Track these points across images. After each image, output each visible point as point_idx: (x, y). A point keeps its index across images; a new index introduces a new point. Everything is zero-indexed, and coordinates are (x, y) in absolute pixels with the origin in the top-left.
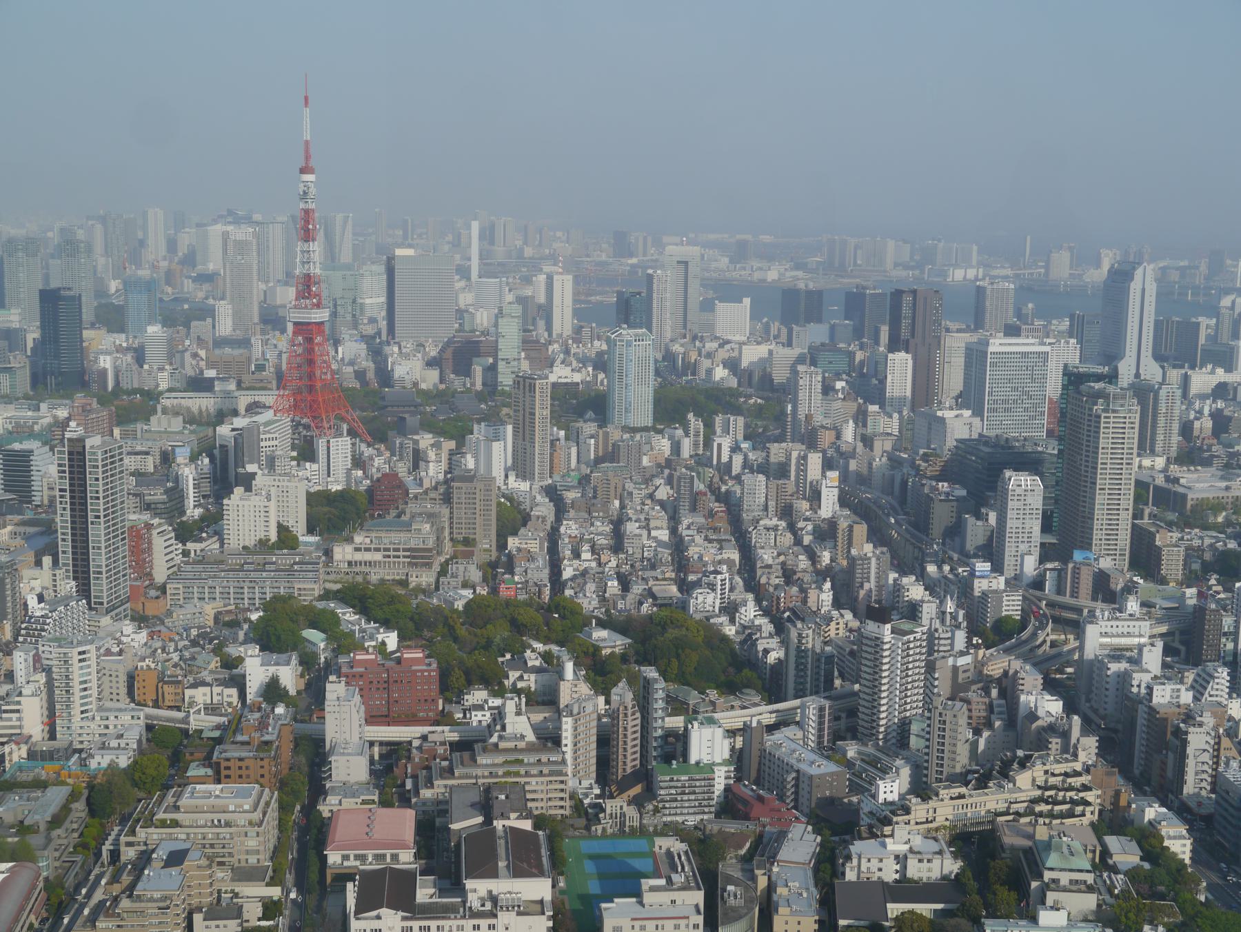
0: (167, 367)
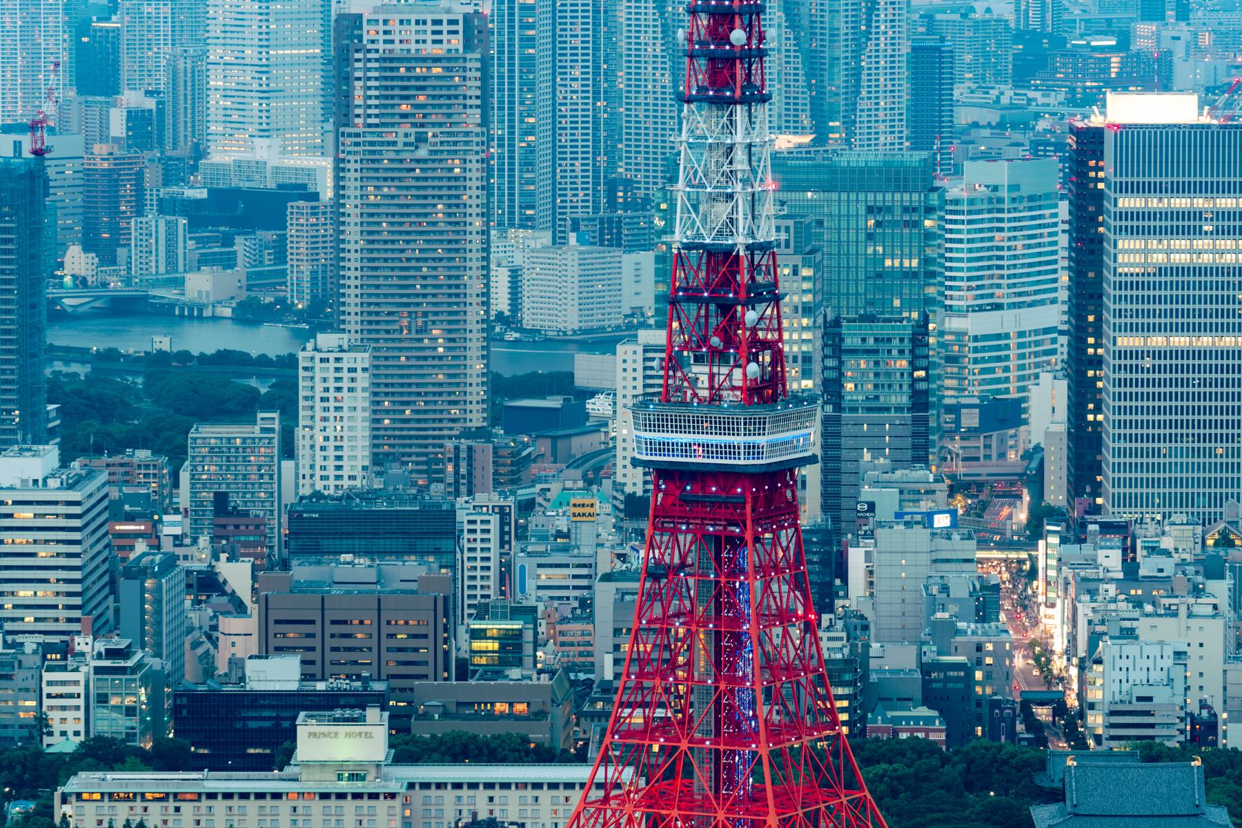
0: (83, 643)
